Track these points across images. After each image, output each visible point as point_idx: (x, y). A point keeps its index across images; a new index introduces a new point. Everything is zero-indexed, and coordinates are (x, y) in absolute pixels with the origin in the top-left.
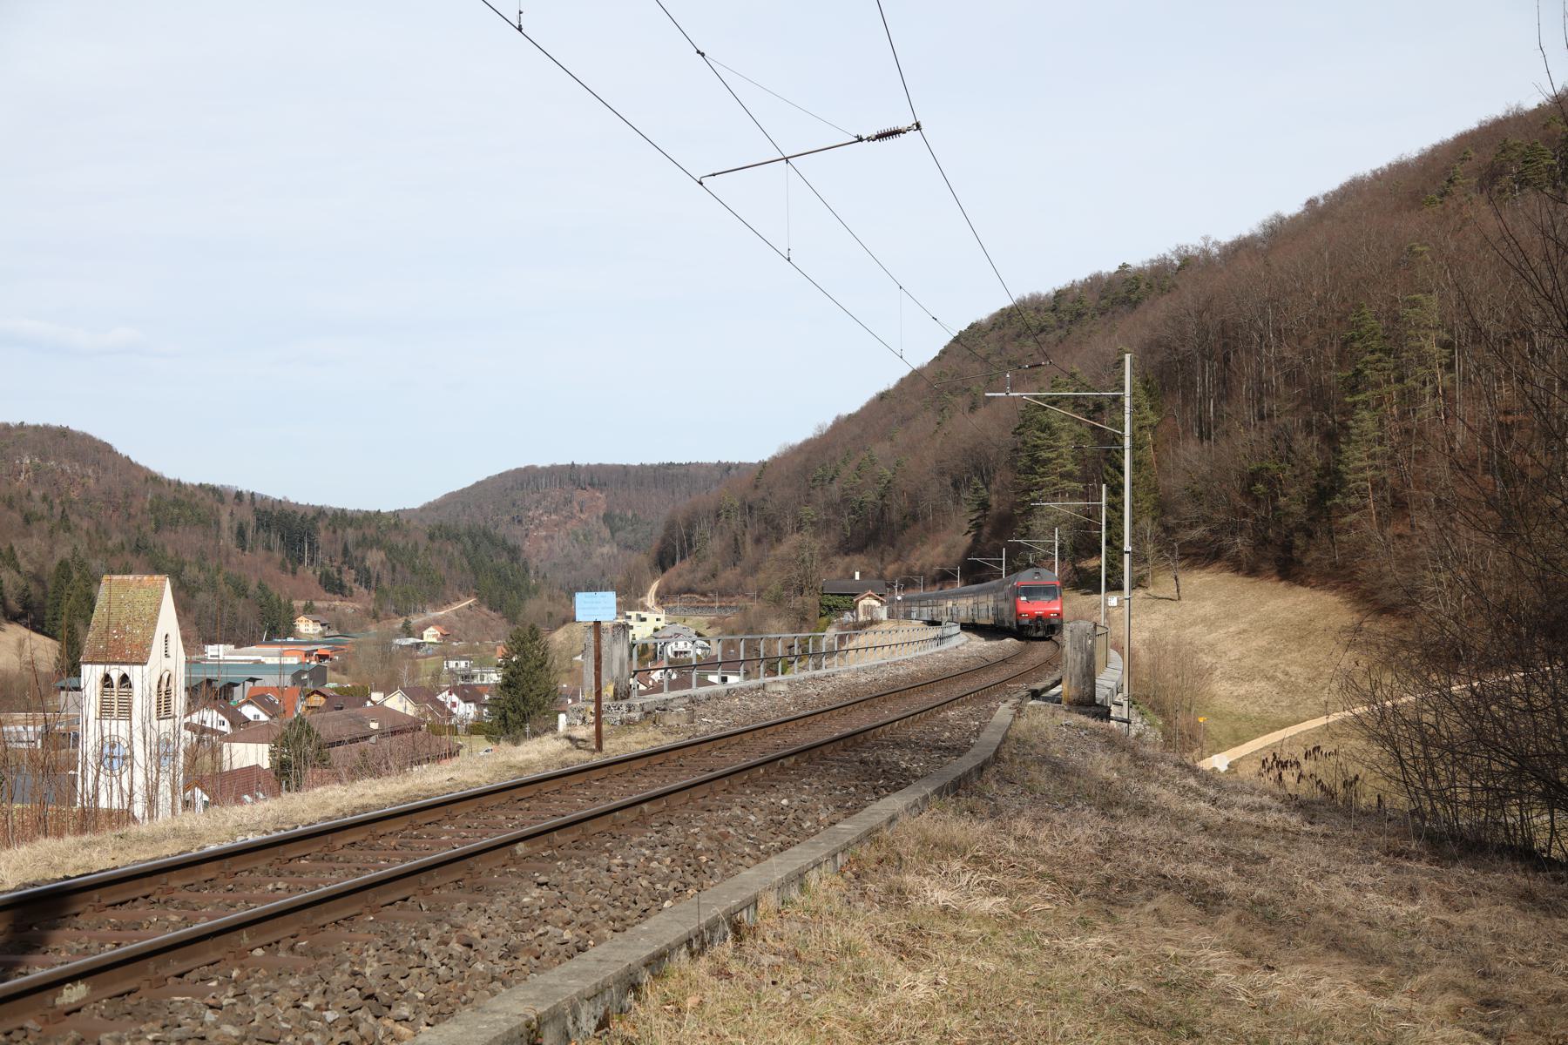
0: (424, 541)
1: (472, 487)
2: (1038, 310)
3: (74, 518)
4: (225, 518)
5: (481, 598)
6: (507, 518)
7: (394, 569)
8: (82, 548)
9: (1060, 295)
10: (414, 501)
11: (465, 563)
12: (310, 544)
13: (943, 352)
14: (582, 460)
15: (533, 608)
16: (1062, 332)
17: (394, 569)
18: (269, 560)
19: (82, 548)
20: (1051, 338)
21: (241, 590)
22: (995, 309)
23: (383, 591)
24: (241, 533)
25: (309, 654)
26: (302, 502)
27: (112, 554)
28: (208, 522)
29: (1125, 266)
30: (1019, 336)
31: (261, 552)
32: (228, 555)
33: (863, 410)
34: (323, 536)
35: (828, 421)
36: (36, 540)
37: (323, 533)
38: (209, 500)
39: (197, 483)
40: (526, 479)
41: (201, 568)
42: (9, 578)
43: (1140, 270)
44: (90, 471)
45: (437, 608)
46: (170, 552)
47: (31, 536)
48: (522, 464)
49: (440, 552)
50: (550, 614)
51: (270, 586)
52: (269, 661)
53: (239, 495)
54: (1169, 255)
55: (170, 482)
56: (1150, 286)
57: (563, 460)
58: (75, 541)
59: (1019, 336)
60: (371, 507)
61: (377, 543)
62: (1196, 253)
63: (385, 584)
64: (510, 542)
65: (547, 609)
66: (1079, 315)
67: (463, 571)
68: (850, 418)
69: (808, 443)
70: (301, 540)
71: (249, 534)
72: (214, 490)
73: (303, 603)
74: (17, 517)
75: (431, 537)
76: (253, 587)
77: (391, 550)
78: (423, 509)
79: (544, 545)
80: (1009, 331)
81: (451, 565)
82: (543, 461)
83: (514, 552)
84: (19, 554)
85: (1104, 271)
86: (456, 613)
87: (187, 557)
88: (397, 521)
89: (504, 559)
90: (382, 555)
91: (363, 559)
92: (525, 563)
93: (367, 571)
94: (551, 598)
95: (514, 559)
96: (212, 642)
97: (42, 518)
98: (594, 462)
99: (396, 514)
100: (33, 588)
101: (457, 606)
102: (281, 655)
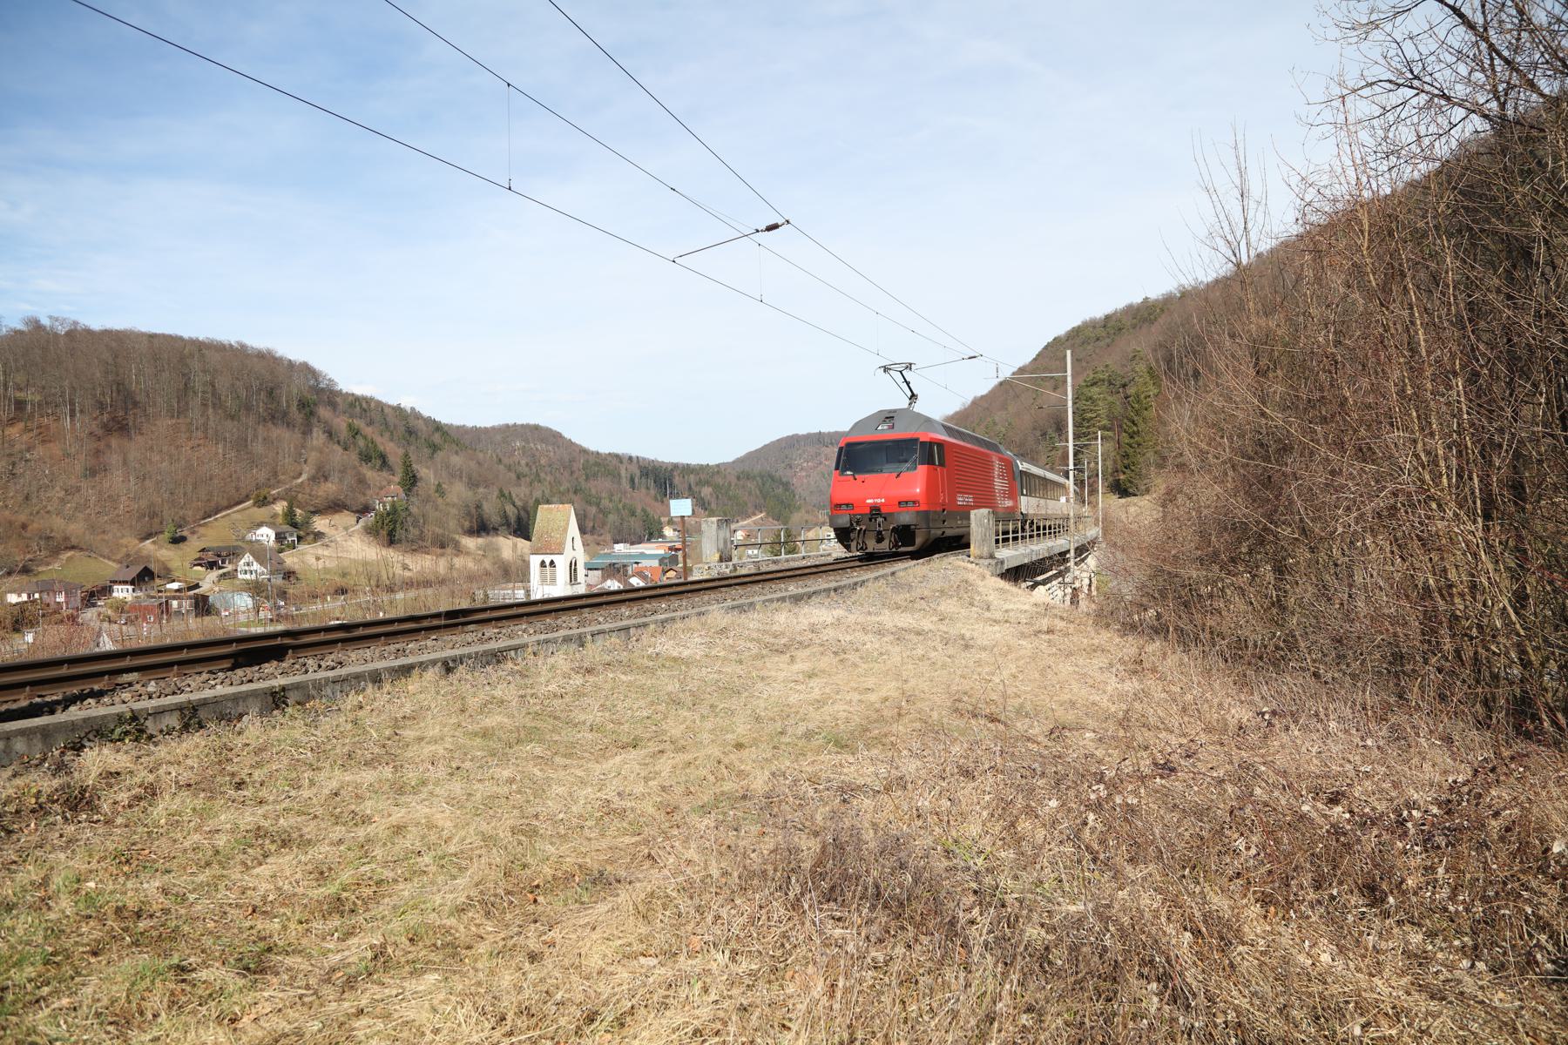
0: (734, 481)
1: (763, 448)
2: (1094, 327)
3: (542, 475)
4: (623, 473)
5: (768, 514)
6: (783, 465)
7: (717, 497)
8: (547, 492)
9: (1108, 318)
10: (730, 458)
11: (758, 492)
12: (671, 485)
13: (1038, 355)
14: (825, 430)
15: (796, 518)
16: (1108, 340)
17: (717, 497)
18: (648, 494)
19: (547, 492)
20: (1102, 344)
21: (633, 514)
22: (1069, 328)
23: (712, 510)
24: (632, 480)
25: (671, 549)
26: (666, 460)
27: (563, 494)
28: (615, 476)
29: (1147, 298)
30: (1083, 343)
31: (644, 490)
32: (625, 492)
33: (991, 392)
34: (677, 480)
35: (969, 400)
36: (523, 488)
37: (677, 478)
38: (615, 462)
39: (607, 452)
40: (792, 444)
41: (611, 501)
42: (511, 510)
43: (1156, 300)
44: (550, 448)
45: (744, 519)
46: (593, 491)
47: (520, 485)
48: (790, 433)
49: (743, 487)
50: (807, 521)
51: (648, 509)
52: (648, 552)
53: (630, 458)
54: (1173, 290)
55: (593, 453)
56: (1162, 310)
57: (814, 429)
58: (543, 488)
59: (1083, 343)
60: (704, 463)
61: (708, 483)
62: (1190, 288)
63: (713, 506)
64: (784, 480)
65: (805, 518)
66: (1120, 329)
67: (757, 497)
68: (982, 397)
69: (957, 413)
70: (665, 483)
71: (636, 481)
72: (617, 456)
73: (667, 519)
74: (513, 476)
75: (738, 478)
76: (639, 511)
77: (716, 487)
78: (734, 462)
79: (805, 481)
80: (1078, 341)
81: (750, 494)
82: (802, 431)
83: (786, 486)
84: (514, 496)
85: (1135, 302)
86: (755, 523)
87: (604, 495)
88: (718, 470)
89: (780, 490)
90: (710, 489)
91: (700, 492)
92: (793, 491)
93: (702, 499)
94: (808, 512)
95: (787, 490)
96: (617, 542)
97: (525, 476)
98: (832, 430)
99: (718, 466)
100: (522, 513)
101: (754, 518)
102: (657, 548)
